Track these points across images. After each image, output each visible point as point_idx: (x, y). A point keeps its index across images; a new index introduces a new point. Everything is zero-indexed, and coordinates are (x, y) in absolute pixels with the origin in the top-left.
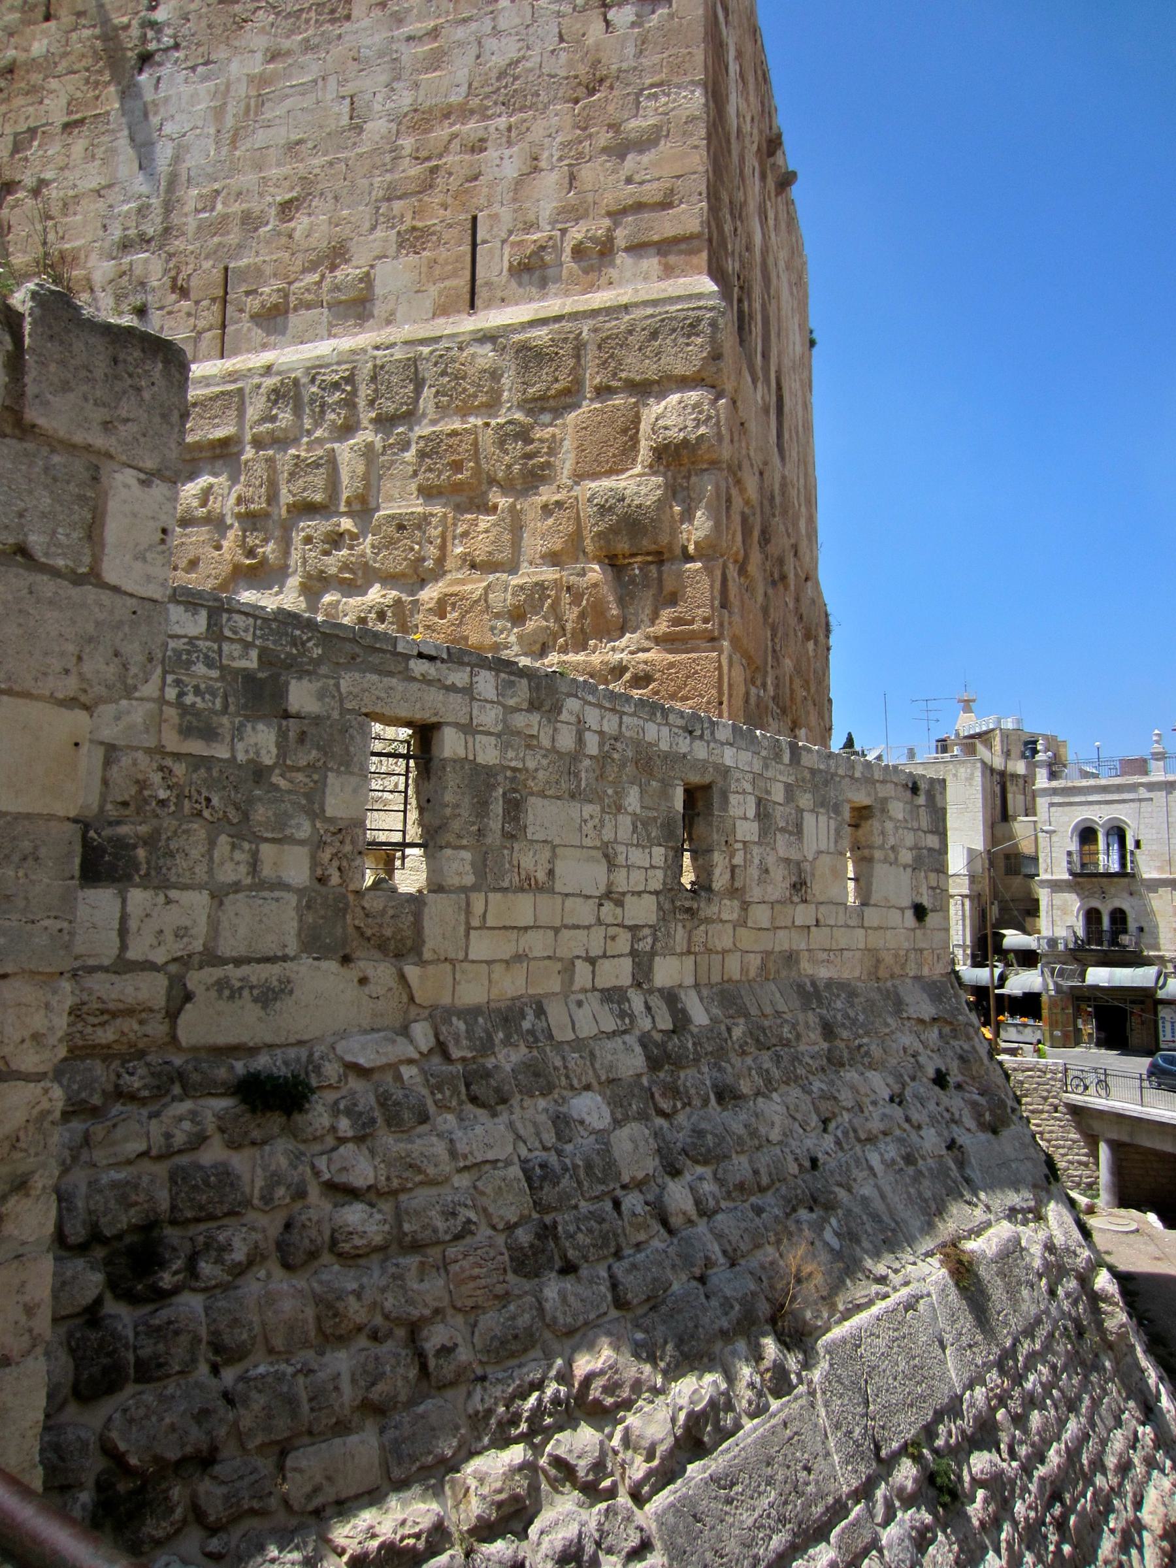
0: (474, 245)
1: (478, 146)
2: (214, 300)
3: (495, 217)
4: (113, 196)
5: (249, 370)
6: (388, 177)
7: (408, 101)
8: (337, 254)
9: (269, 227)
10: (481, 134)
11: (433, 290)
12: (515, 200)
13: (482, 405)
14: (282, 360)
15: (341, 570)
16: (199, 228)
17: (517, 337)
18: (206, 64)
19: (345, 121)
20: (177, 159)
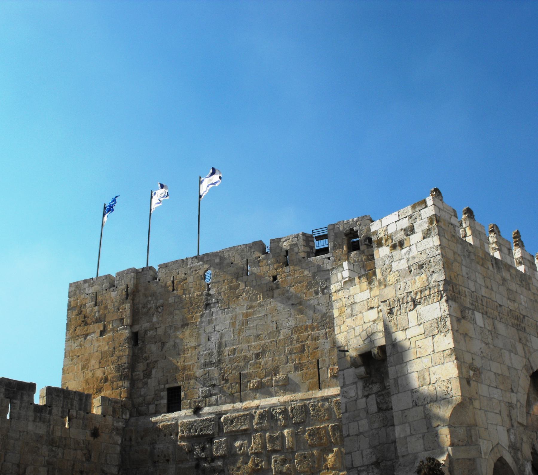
0: (319, 369)
1: (317, 338)
2: (237, 383)
3: (324, 361)
4: (200, 348)
5: (252, 407)
6: (290, 347)
7: (294, 324)
8: (276, 371)
9: (253, 361)
10: (317, 335)
11: (307, 382)
12: (330, 355)
13: (326, 419)
14: (262, 404)
15: (287, 470)
16: (230, 360)
17: (334, 399)
18: (228, 308)
19: (275, 329)
20: (221, 338)
